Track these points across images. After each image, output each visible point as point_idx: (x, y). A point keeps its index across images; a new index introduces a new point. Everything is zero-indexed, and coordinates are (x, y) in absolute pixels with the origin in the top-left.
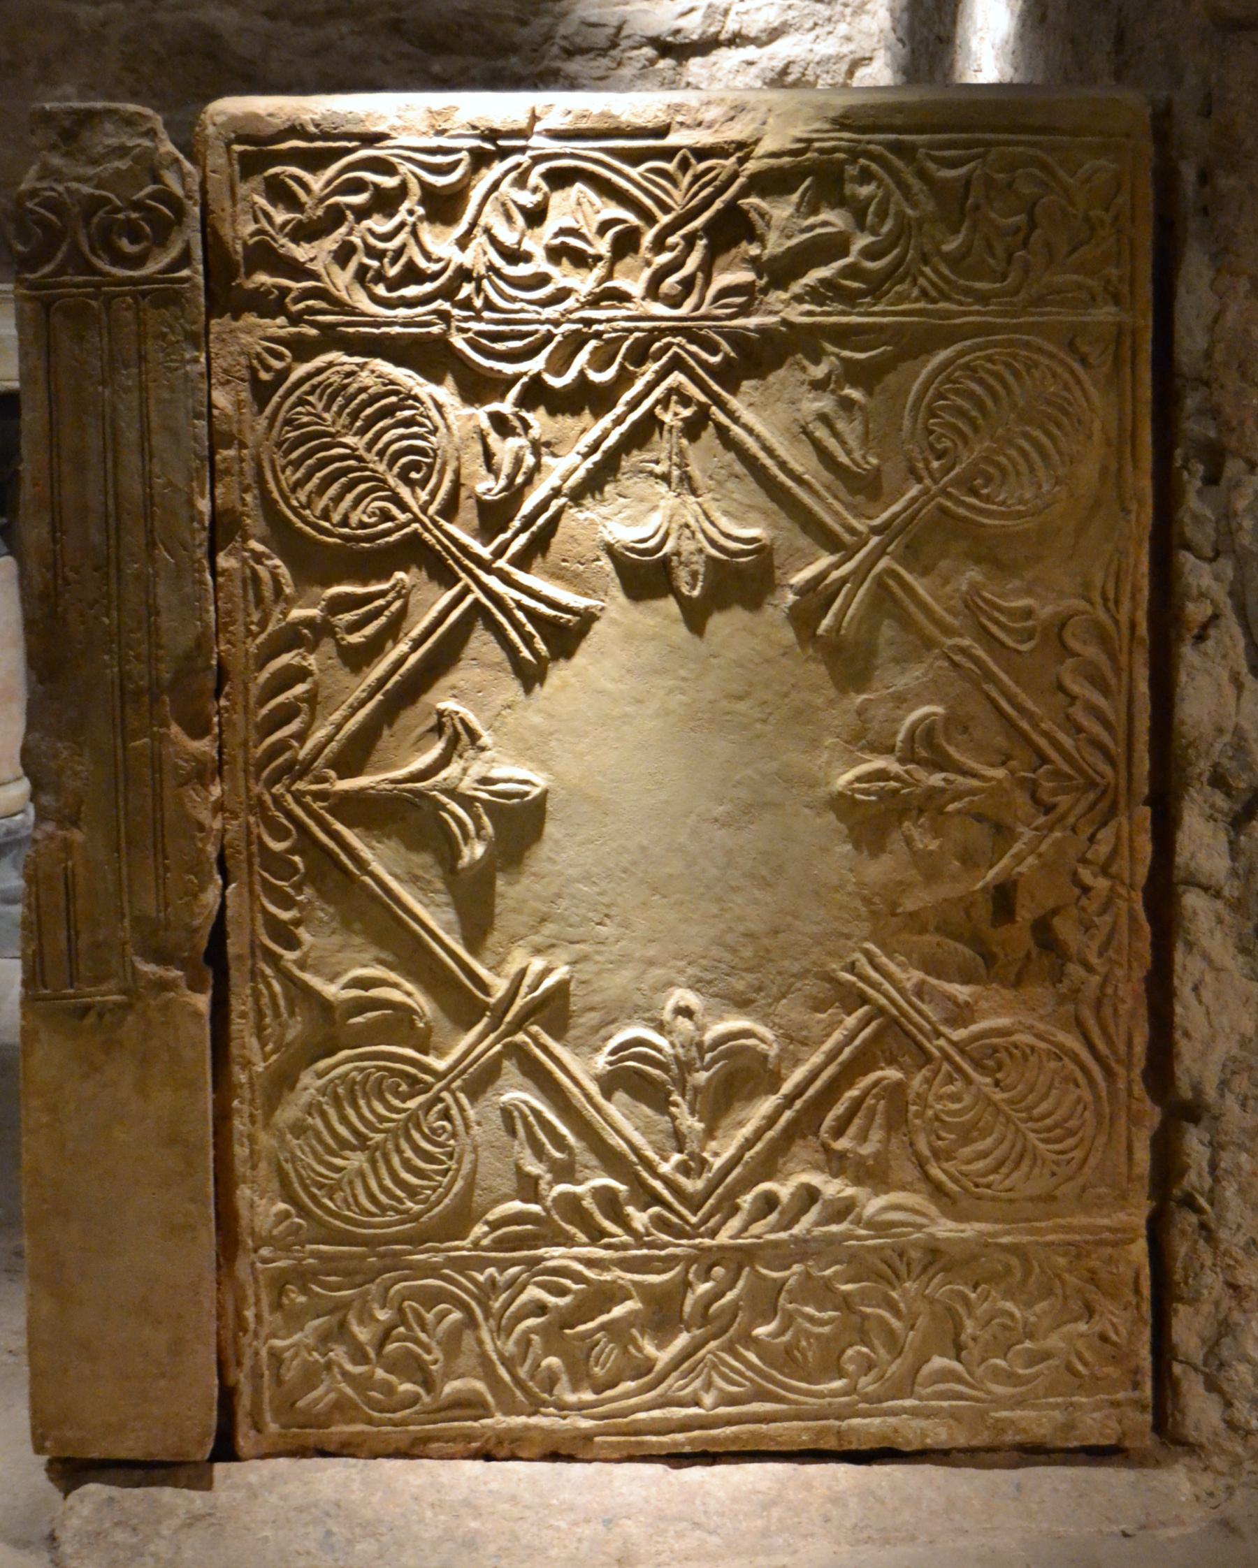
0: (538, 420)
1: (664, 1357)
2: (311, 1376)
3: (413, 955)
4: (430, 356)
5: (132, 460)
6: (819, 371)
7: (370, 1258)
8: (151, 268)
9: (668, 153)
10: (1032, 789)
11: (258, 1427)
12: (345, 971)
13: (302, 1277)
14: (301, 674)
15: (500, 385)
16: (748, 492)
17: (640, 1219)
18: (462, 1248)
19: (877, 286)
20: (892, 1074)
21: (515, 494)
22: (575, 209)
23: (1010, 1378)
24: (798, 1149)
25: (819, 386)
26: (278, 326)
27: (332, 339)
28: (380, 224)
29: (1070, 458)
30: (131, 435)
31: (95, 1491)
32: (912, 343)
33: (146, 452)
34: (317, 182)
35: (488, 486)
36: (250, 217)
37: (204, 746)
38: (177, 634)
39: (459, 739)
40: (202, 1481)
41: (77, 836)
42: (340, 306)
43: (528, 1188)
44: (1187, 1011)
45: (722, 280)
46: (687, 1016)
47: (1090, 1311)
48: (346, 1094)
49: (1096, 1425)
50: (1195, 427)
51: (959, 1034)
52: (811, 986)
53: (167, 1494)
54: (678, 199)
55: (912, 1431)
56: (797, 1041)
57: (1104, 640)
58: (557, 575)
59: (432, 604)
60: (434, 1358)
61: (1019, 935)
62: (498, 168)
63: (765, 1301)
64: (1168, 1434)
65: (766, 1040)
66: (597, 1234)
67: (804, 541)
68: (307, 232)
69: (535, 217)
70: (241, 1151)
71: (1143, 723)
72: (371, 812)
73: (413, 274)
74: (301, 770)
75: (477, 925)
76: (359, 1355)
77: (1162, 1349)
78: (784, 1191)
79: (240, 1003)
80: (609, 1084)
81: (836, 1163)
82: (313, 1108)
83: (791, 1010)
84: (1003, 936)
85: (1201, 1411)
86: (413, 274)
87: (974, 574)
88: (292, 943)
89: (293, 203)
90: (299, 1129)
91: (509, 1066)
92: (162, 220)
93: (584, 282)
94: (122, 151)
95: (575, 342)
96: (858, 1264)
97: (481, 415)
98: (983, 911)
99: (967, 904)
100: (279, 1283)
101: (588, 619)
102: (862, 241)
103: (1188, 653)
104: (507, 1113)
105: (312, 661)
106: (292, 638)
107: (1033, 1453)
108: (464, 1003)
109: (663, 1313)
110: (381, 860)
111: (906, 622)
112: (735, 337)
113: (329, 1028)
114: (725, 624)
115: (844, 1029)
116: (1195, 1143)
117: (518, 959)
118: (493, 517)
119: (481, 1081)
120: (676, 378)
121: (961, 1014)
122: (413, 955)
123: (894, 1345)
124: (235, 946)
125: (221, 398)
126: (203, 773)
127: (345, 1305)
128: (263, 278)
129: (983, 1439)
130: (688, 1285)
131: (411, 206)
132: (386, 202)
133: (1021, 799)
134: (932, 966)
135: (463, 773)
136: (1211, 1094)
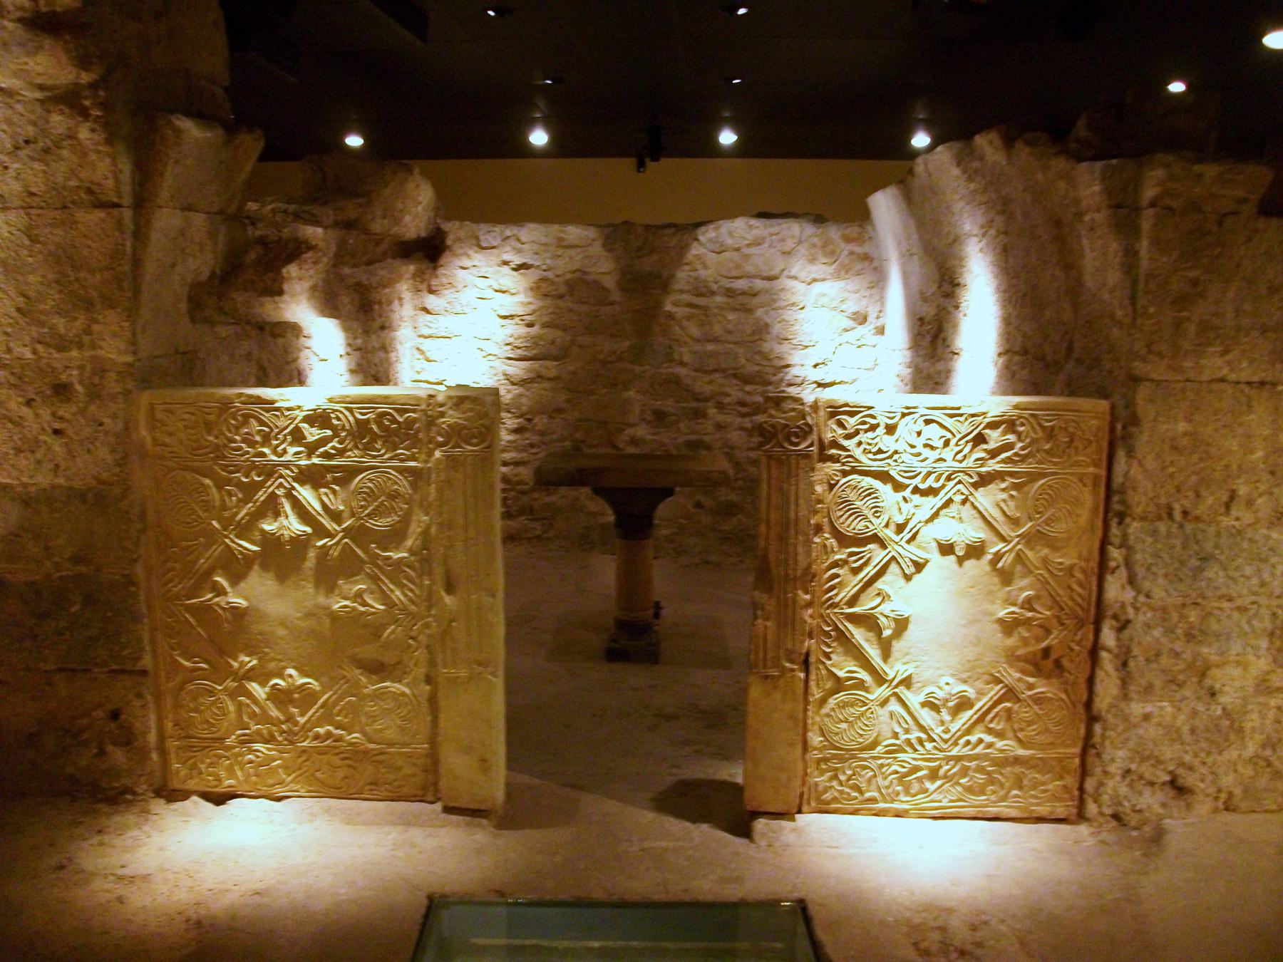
0: (916, 497)
2: (826, 790)
4: (884, 477)
5: (792, 507)
6: (1003, 485)
7: (847, 755)
9: (961, 415)
10: (1057, 617)
11: (809, 803)
12: (844, 667)
13: (825, 760)
14: (837, 576)
17: (929, 746)
18: (875, 753)
19: (1023, 459)
20: (1008, 705)
22: (933, 432)
23: (1036, 797)
24: (980, 727)
25: (1003, 490)
26: (837, 466)
27: (854, 471)
28: (870, 435)
30: (792, 499)
32: (1033, 477)
33: (797, 505)
35: (901, 520)
36: (831, 432)
37: (808, 597)
39: (884, 597)
40: (793, 820)
41: (769, 624)
42: (857, 461)
44: (1099, 688)
47: (1061, 778)
48: (843, 705)
49: (1061, 811)
50: (1117, 507)
51: (1030, 693)
52: (986, 677)
53: (783, 823)
56: (981, 693)
57: (1084, 571)
58: (919, 547)
60: (863, 785)
61: (1049, 664)
62: (907, 418)
63: (964, 772)
64: (1081, 817)
65: (971, 693)
66: (916, 750)
67: (995, 539)
68: (848, 437)
69: (919, 434)
70: (810, 721)
71: (1094, 598)
72: (855, 619)
74: (836, 605)
75: (886, 655)
76: (841, 784)
77: (1081, 789)
79: (813, 677)
80: (924, 705)
81: (990, 731)
82: (833, 710)
83: (979, 684)
84: (1043, 663)
85: (1092, 808)
87: (1046, 551)
88: (830, 659)
89: (845, 428)
90: (828, 715)
91: (893, 699)
93: (933, 455)
94: (794, 410)
96: (995, 762)
97: (899, 496)
98: (1039, 656)
99: (1034, 653)
100: (819, 761)
101: (927, 561)
102: (1020, 445)
103: (1109, 578)
104: (892, 714)
105: (841, 572)
106: (836, 564)
107: (1040, 820)
108: (880, 679)
109: (933, 775)
110: (859, 635)
111: (1025, 565)
112: (979, 474)
113: (839, 685)
114: (969, 564)
115: (996, 691)
116: (1097, 728)
118: (900, 528)
119: (884, 703)
120: (960, 486)
121: (1031, 687)
123: (1002, 786)
124: (812, 659)
125: (819, 489)
126: (809, 604)
127: (836, 769)
128: (833, 451)
129: (1026, 815)
130: (940, 767)
131: (881, 430)
132: (873, 428)
133: (1055, 621)
134: (1023, 672)
135: (886, 608)
136: (1103, 713)
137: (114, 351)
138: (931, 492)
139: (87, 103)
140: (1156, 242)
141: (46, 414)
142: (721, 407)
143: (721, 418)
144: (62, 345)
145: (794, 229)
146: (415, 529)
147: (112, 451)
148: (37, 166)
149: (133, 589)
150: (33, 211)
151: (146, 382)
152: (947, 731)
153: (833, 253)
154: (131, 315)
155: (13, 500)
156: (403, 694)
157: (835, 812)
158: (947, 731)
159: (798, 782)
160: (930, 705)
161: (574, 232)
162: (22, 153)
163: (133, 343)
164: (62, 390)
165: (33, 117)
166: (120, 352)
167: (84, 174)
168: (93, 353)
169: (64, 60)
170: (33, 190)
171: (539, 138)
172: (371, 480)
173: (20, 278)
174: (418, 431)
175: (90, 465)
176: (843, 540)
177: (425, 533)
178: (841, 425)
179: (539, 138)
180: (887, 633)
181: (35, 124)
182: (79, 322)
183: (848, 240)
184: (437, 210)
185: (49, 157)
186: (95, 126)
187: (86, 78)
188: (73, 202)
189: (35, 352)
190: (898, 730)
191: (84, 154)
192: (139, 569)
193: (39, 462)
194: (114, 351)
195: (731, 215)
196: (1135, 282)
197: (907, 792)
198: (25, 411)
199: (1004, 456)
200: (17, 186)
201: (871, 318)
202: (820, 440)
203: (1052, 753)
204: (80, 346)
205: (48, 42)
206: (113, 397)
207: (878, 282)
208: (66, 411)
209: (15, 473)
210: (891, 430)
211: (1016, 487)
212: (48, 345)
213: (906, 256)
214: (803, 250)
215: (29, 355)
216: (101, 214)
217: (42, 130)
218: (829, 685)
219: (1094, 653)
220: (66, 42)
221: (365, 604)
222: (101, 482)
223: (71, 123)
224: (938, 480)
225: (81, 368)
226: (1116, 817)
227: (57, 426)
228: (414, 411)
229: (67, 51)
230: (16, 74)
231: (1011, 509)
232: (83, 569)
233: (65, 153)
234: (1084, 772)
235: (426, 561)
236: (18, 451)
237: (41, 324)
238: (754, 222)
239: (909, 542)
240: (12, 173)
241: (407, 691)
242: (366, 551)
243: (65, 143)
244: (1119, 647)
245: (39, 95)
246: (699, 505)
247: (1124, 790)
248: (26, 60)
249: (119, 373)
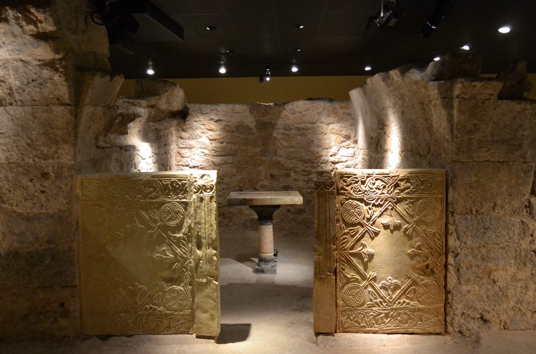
0: (374, 208)
1: (387, 321)
2: (345, 323)
3: (358, 272)
4: (361, 200)
5: (328, 213)
6: (407, 202)
7: (353, 309)
8: (330, 190)
9: (389, 177)
10: (431, 253)
11: (339, 329)
12: (351, 274)
13: (345, 311)
14: (346, 238)
15: (369, 204)
16: (398, 217)
17: (384, 304)
18: (363, 308)
19: (414, 192)
20: (414, 287)
21: (371, 217)
22: (379, 183)
23: (428, 324)
24: (403, 296)
25: (407, 204)
26: (344, 197)
27: (350, 198)
28: (356, 185)
29: (436, 214)
30: (328, 210)
31: (321, 337)
32: (418, 199)
33: (329, 211)
34: (349, 180)
35: (368, 216)
37: (335, 247)
38: (333, 234)
39: (364, 246)
40: (333, 335)
41: (320, 257)
43: (371, 300)
44: (449, 280)
45: (395, 192)
46: (391, 280)
47: (437, 316)
48: (351, 289)
49: (438, 330)
50: (450, 209)
51: (422, 282)
52: (405, 276)
53: (330, 337)
54: (391, 182)
55: (416, 331)
56: (403, 283)
57: (440, 235)
59: (361, 230)
60: (360, 321)
61: (429, 271)
62: (370, 178)
63: (399, 314)
64: (446, 332)
65: (399, 283)
67: (405, 223)
68: (348, 186)
69: (374, 184)
70: (338, 296)
71: (444, 245)
73: (360, 191)
74: (345, 250)
75: (366, 269)
76: (351, 320)
78: (401, 301)
79: (338, 278)
80: (381, 288)
81: (407, 298)
82: (346, 290)
83: (402, 279)
84: (428, 271)
85: (450, 329)
86: (360, 191)
87: (424, 227)
88: (344, 270)
89: (346, 182)
90: (345, 293)
91: (369, 286)
93: (380, 192)
94: (327, 176)
95: (378, 199)
96: (410, 310)
97: (367, 207)
98: (425, 268)
99: (422, 267)
100: (342, 312)
101: (379, 232)
102: (412, 187)
103: (449, 237)
104: (369, 291)
105: (347, 237)
107: (430, 334)
108: (364, 278)
109: (387, 316)
110: (355, 261)
111: (417, 233)
112: (397, 198)
113: (348, 281)
114: (395, 233)
115: (409, 282)
116: (450, 296)
117: (371, 273)
118: (368, 220)
119: (366, 287)
121: (422, 280)
122: (358, 272)
123: (414, 320)
124: (338, 271)
125: (337, 205)
126: (336, 249)
127: (349, 315)
128: (342, 191)
129: (425, 332)
130: (390, 312)
131: (359, 183)
132: (357, 182)
133: (430, 254)
135: (365, 250)
136: (452, 290)
137: (66, 159)
138: (380, 206)
139: (58, 66)
140: (459, 111)
141: (38, 185)
144: (46, 158)
146: (186, 225)
147: (66, 198)
148: (37, 89)
149: (72, 253)
150: (35, 107)
151: (79, 171)
152: (391, 298)
154: (74, 145)
155: (23, 219)
156: (181, 290)
158: (391, 298)
159: (334, 320)
160: (384, 288)
161: (238, 107)
162: (31, 85)
163: (75, 156)
164: (45, 175)
165: (36, 71)
166: (69, 160)
167: (56, 93)
168: (58, 161)
169: (49, 50)
170: (35, 98)
171: (223, 71)
172: (168, 207)
173: (29, 132)
174: (187, 187)
175: (56, 205)
176: (348, 225)
177: (190, 227)
178: (345, 181)
179: (223, 71)
180: (366, 260)
181: (36, 74)
182: (52, 149)
185: (42, 86)
186: (61, 75)
187: (57, 57)
188: (51, 103)
189: (34, 161)
190: (372, 298)
191: (57, 85)
192: (75, 245)
193: (34, 204)
194: (66, 159)
197: (377, 323)
198: (29, 184)
199: (406, 191)
200: (28, 98)
202: (337, 187)
203: (433, 306)
204: (53, 158)
205: (42, 43)
206: (66, 178)
209: (24, 208)
210: (363, 183)
211: (411, 203)
212: (39, 158)
215: (31, 161)
216: (62, 108)
217: (39, 76)
218: (344, 281)
219: (446, 266)
220: (50, 44)
221: (166, 255)
222: (59, 210)
223: (51, 74)
224: (381, 201)
225: (53, 167)
226: (460, 332)
227: (43, 189)
228: (185, 180)
229: (51, 47)
230: (29, 55)
231: (410, 211)
232: (51, 246)
233: (48, 85)
234: (446, 314)
235: (189, 237)
236: (26, 200)
237: (36, 150)
239: (372, 225)
240: (26, 92)
241: (182, 289)
242: (167, 234)
243: (49, 81)
244: (456, 264)
245: (38, 63)
247: (462, 321)
248: (34, 50)
249: (69, 168)
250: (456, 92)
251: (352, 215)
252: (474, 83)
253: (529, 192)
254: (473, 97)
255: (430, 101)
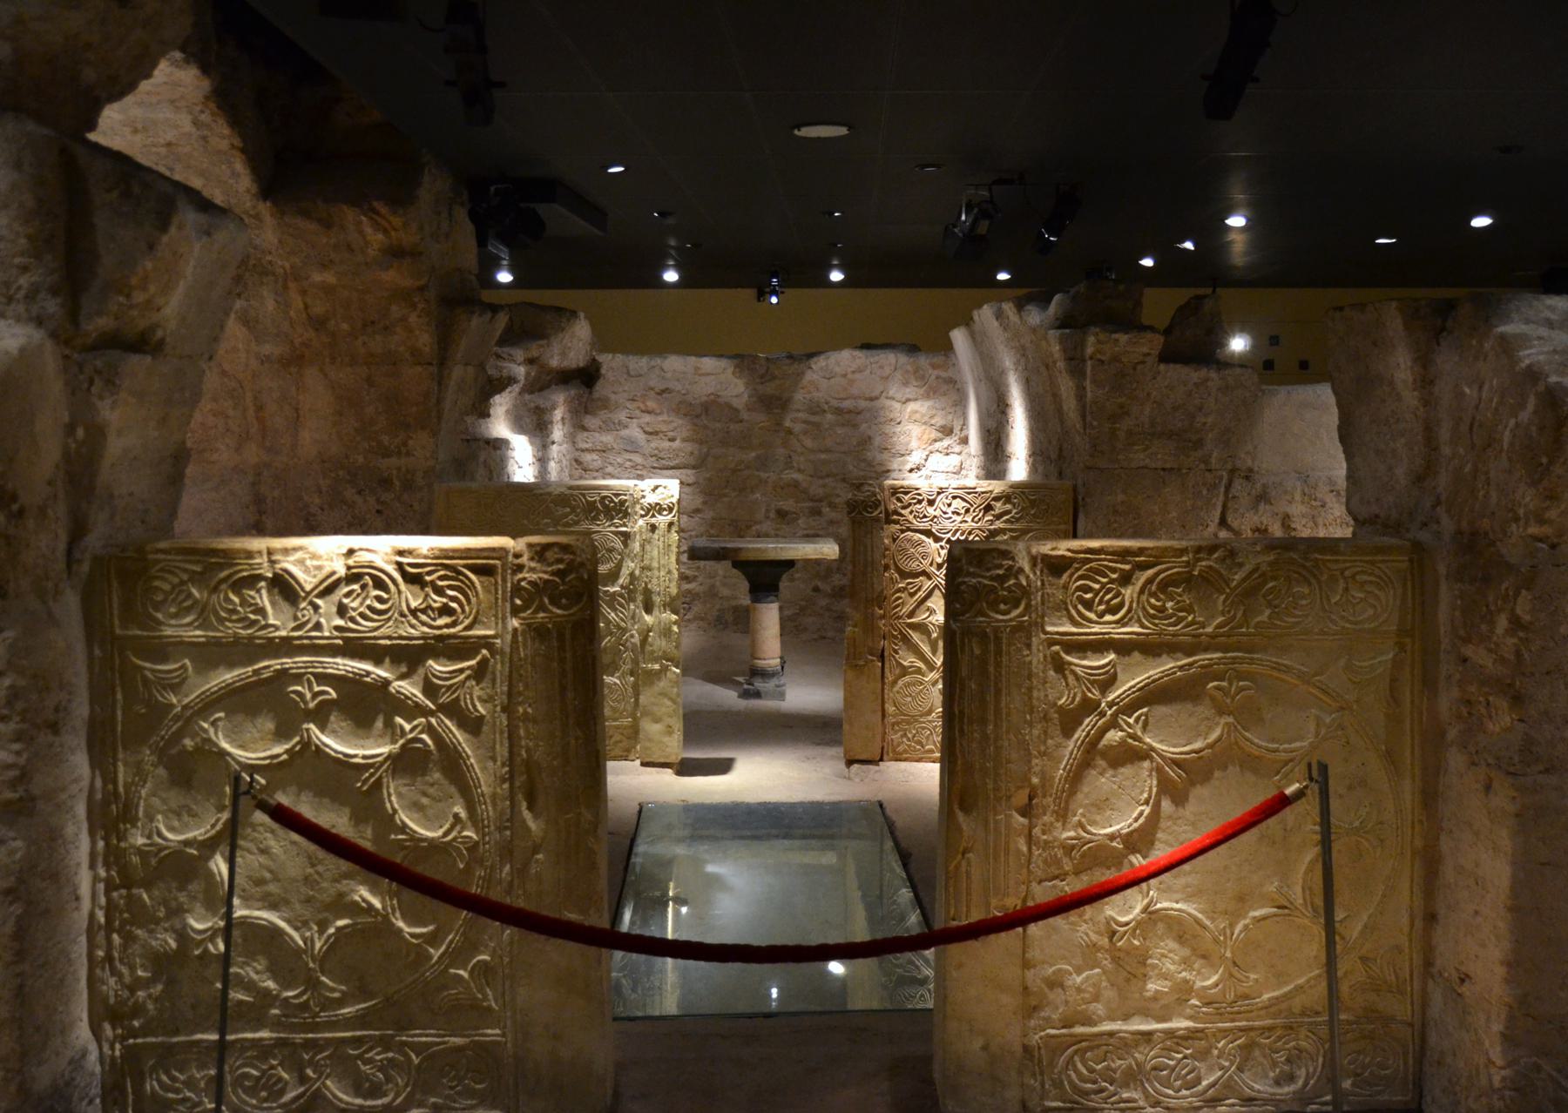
4: (928, 533)
12: (909, 660)
13: (898, 723)
19: (1017, 520)
27: (909, 529)
31: (856, 766)
36: (894, 505)
38: (878, 588)
48: (908, 685)
59: (928, 584)
68: (904, 508)
74: (899, 618)
92: (877, 504)
93: (959, 519)
106: (899, 590)
110: (916, 637)
113: (905, 671)
126: (883, 617)
132: (920, 502)
140: (1094, 381)
141: (372, 500)
142: (832, 506)
143: (833, 515)
145: (889, 359)
146: (625, 572)
153: (923, 377)
157: (905, 760)
159: (879, 738)
176: (904, 575)
177: (632, 574)
178: (899, 500)
183: (934, 367)
184: (593, 345)
195: (838, 347)
196: (1084, 407)
201: (957, 430)
204: (399, 453)
207: (960, 404)
208: (387, 497)
210: (931, 503)
213: (978, 381)
214: (898, 375)
215: (361, 459)
216: (419, 369)
235: (630, 592)
238: (857, 353)
246: (816, 589)
250: (1089, 350)
251: (911, 557)
252: (1115, 336)
253: (1217, 521)
254: (1116, 359)
255: (1055, 362)
